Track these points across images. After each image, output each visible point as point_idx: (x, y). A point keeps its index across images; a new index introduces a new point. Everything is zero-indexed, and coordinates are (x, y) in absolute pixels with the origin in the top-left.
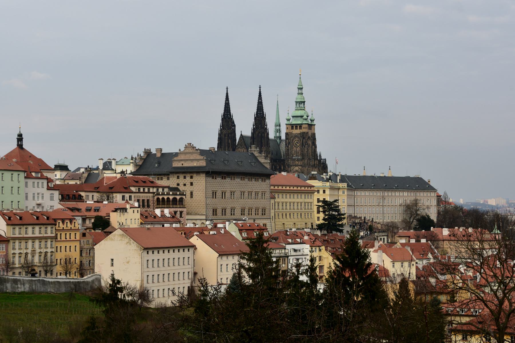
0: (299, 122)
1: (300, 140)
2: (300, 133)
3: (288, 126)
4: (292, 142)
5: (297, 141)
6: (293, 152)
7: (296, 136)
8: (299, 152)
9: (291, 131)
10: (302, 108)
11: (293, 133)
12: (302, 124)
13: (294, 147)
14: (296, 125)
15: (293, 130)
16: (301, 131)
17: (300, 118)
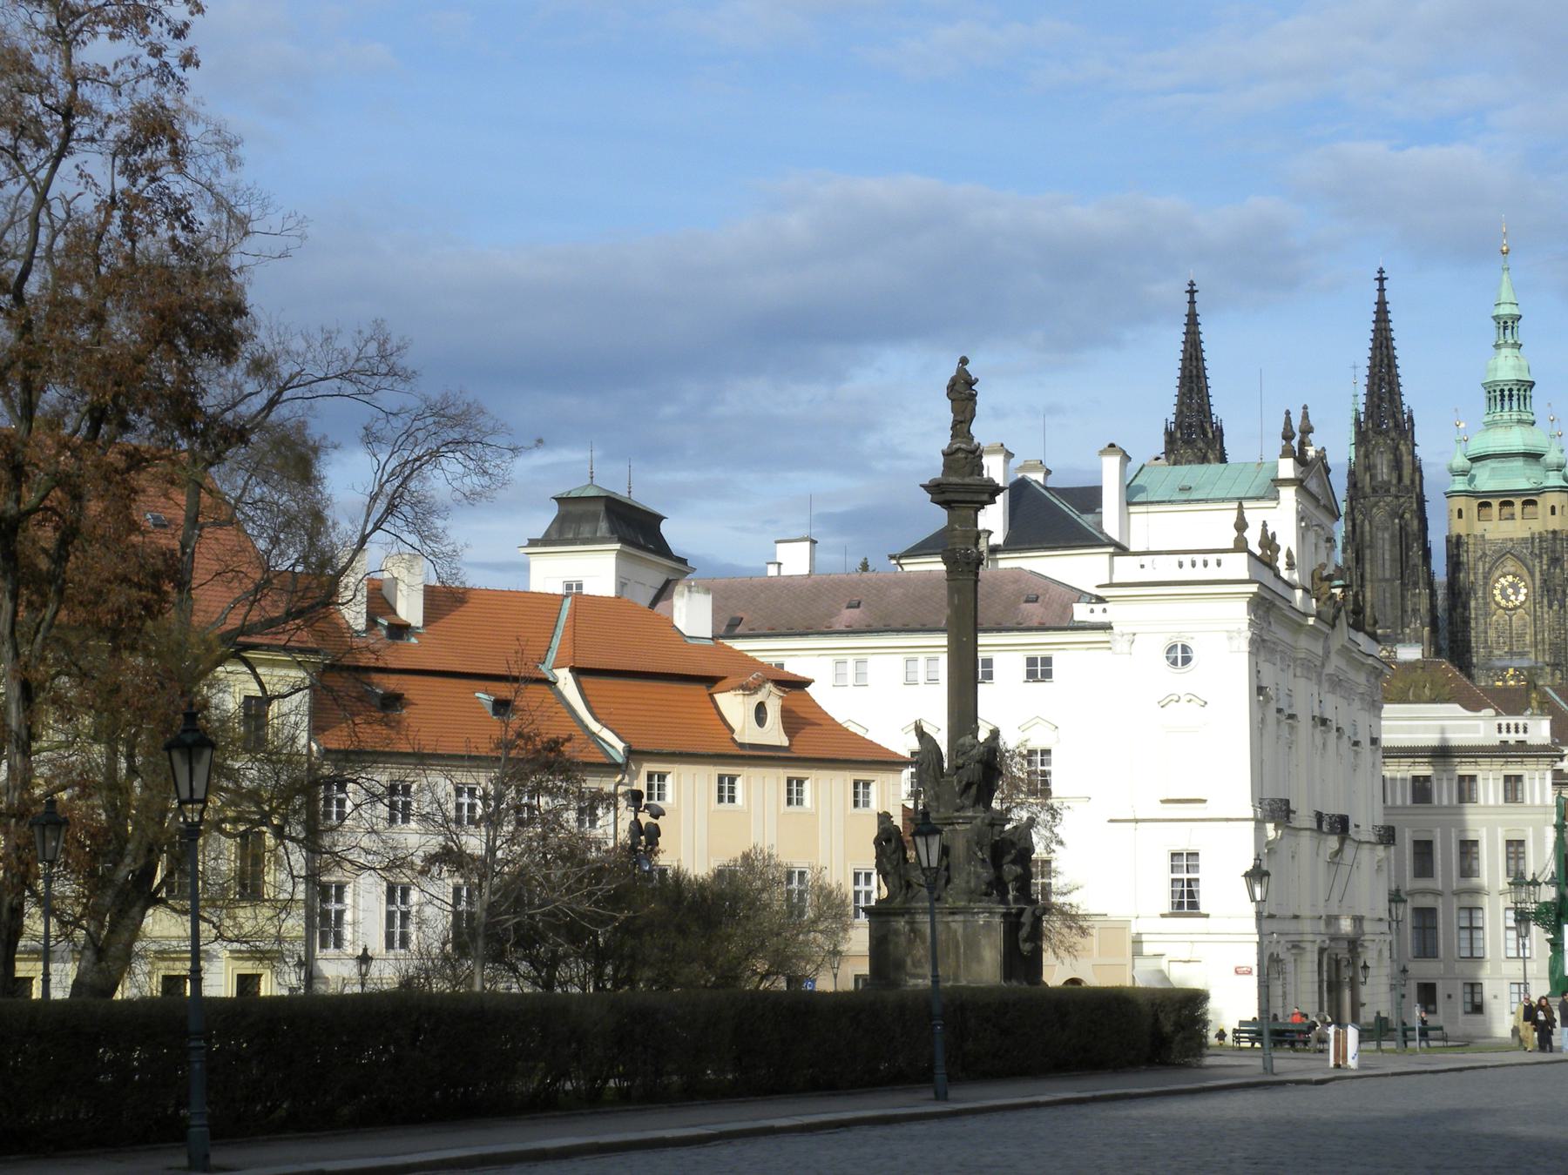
0: (1522, 484)
1: (1532, 574)
2: (1527, 535)
3: (1460, 502)
4: (1486, 584)
5: (1510, 578)
6: (1492, 634)
7: (1504, 552)
8: (1521, 636)
9: (1479, 528)
10: (1524, 417)
11: (1487, 536)
12: (1541, 491)
13: (1494, 606)
14: (1506, 499)
15: (1487, 525)
16: (1537, 526)
17: (1519, 463)
